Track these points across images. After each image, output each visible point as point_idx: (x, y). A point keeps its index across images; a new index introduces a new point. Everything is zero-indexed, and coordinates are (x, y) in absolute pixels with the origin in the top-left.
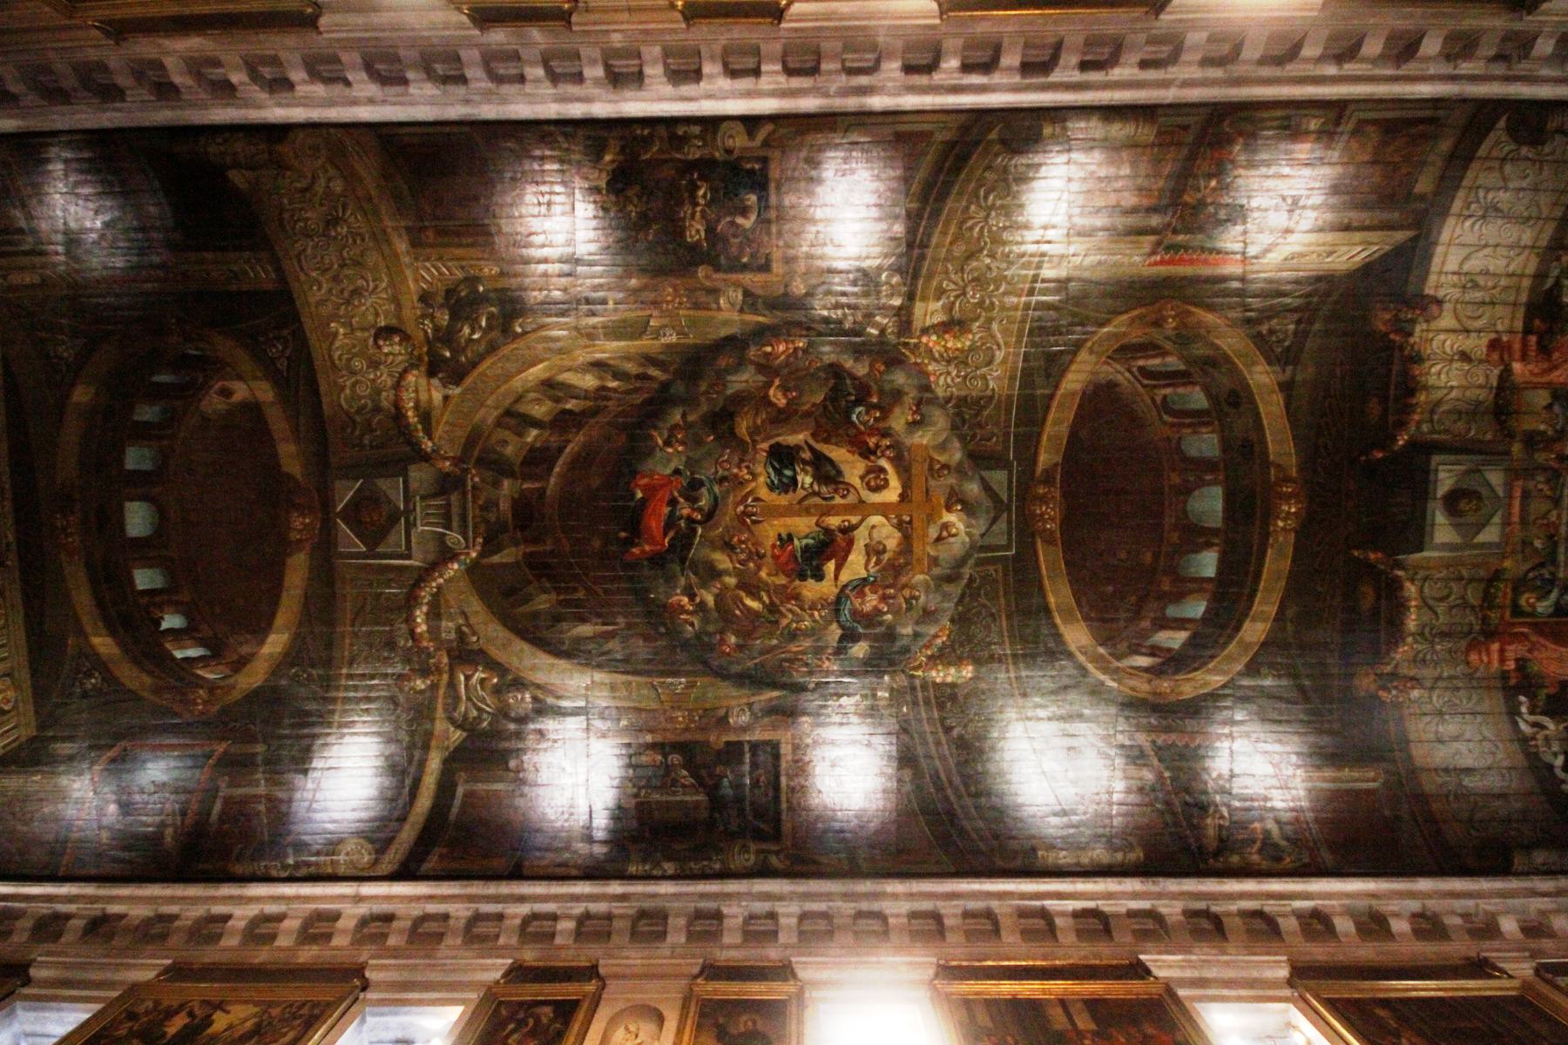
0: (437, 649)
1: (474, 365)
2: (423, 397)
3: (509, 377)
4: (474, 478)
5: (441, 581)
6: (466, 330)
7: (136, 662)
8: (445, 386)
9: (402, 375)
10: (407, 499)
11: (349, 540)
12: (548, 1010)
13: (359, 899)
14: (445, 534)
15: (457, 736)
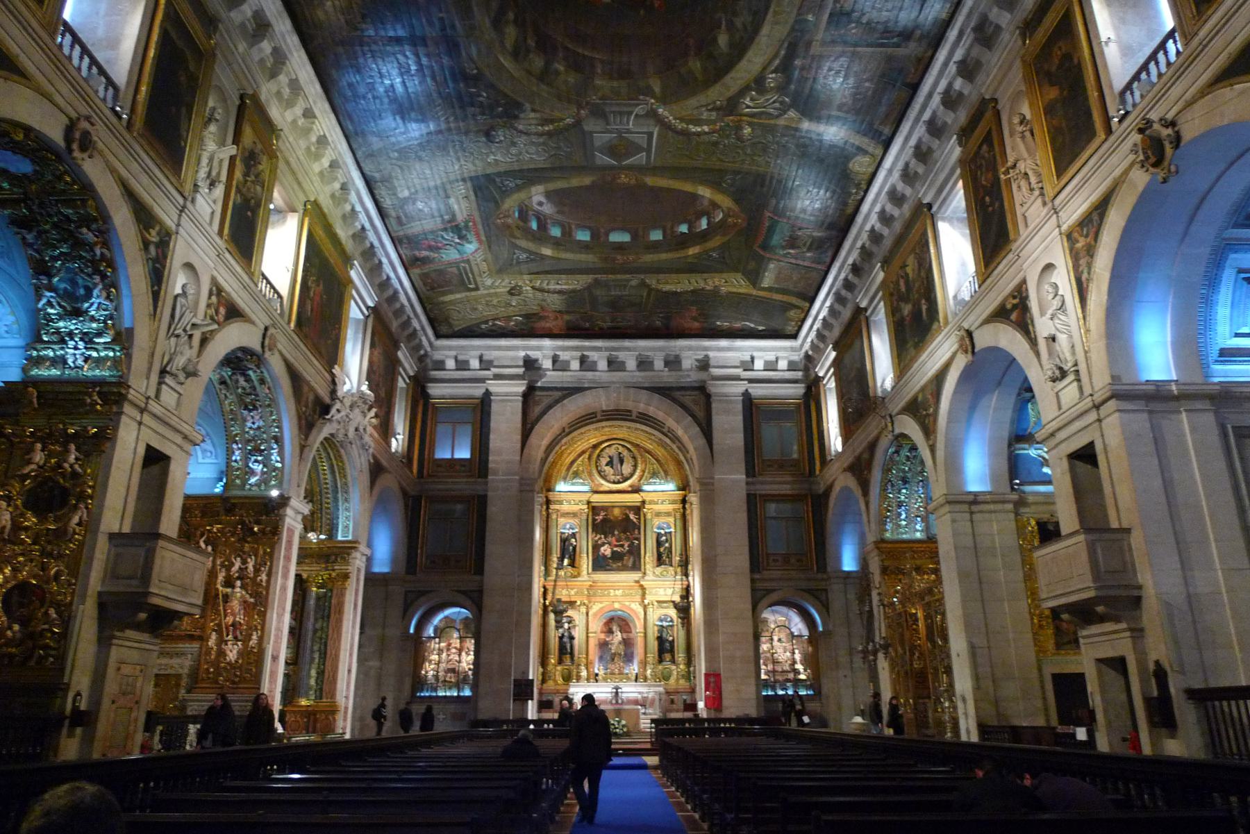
0: (723, 121)
1: (505, 95)
2: (534, 122)
3: (512, 77)
4: (594, 99)
5: (671, 118)
6: (481, 99)
7: (705, 241)
8: (524, 111)
9: (521, 132)
10: (611, 132)
11: (640, 158)
12: (985, 147)
13: (890, 171)
14: (637, 115)
15: (792, 113)
